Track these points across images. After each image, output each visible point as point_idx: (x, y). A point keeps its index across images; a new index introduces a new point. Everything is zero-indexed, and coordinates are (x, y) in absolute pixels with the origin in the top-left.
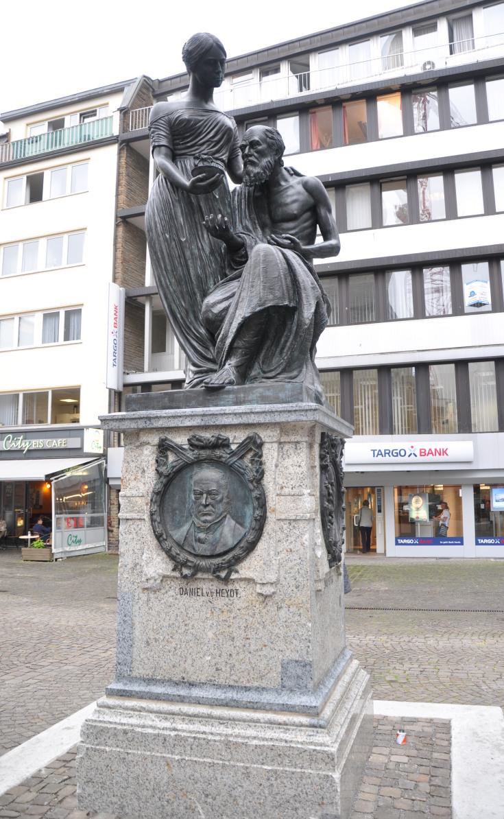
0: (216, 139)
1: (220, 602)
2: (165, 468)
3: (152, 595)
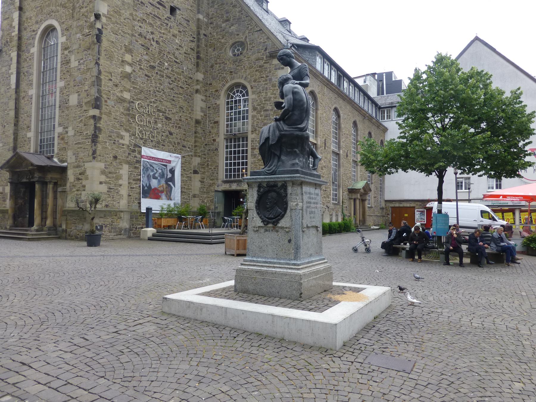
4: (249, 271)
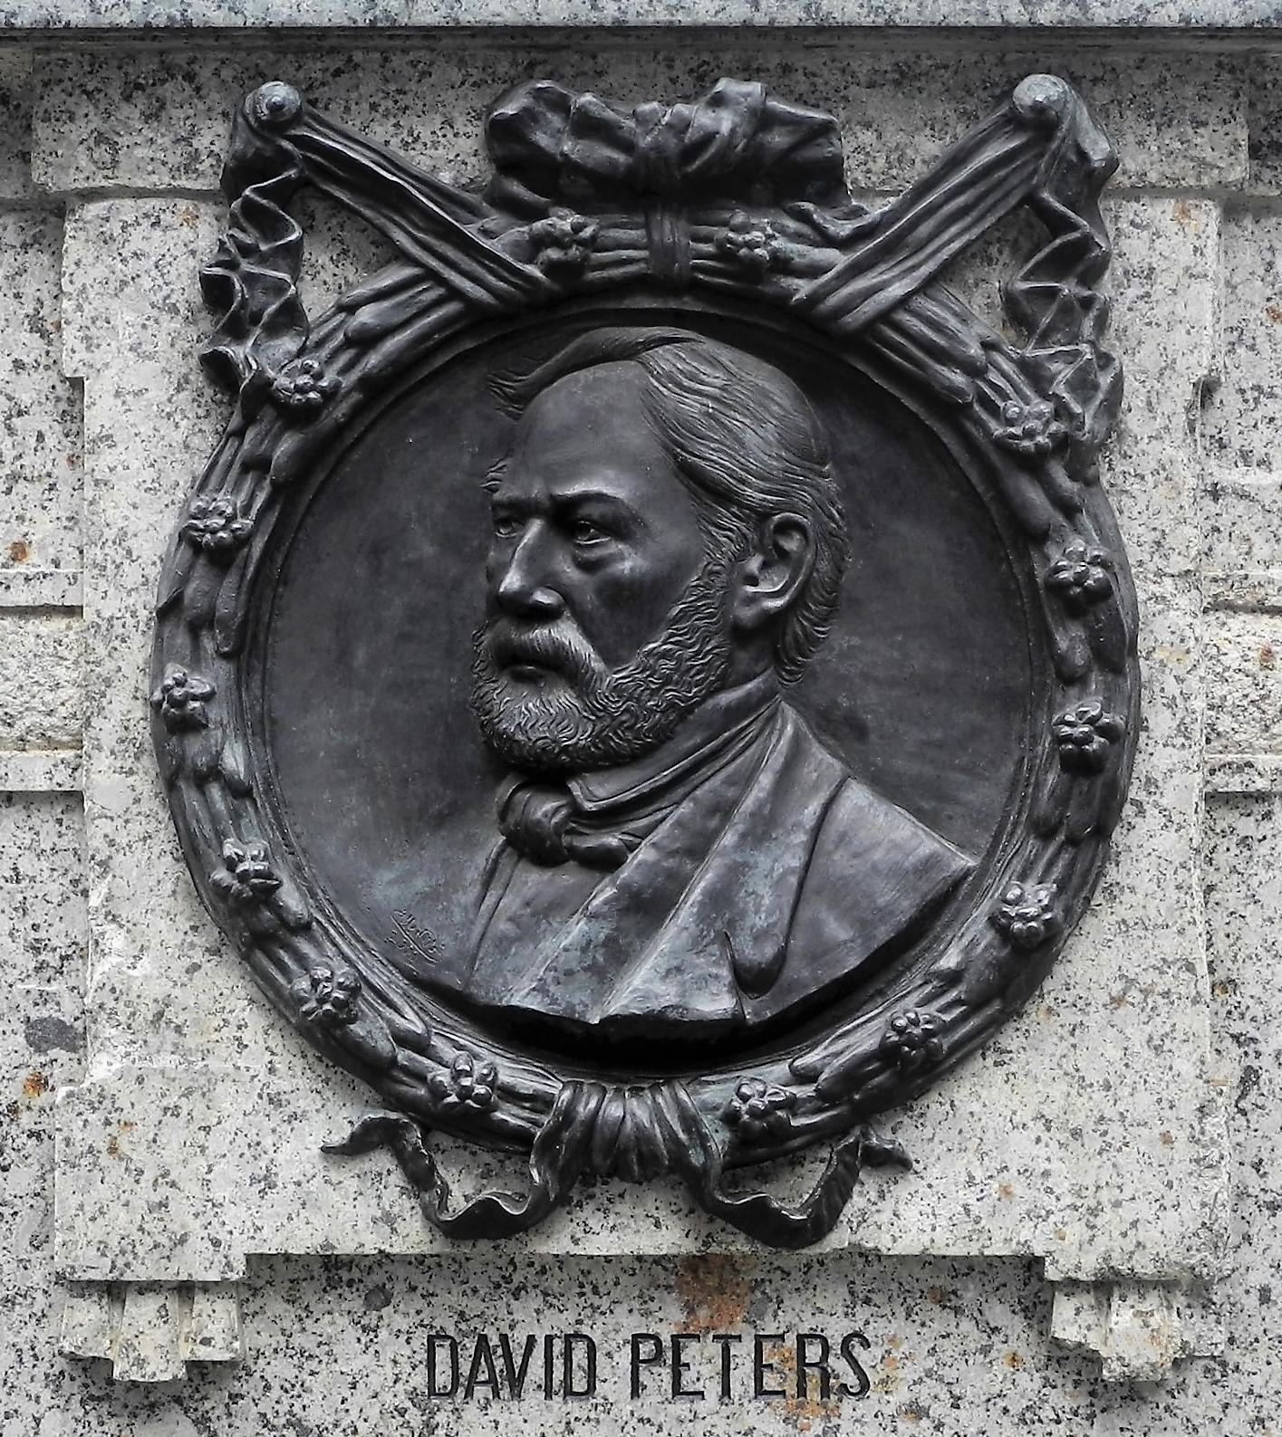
2: (289, 344)
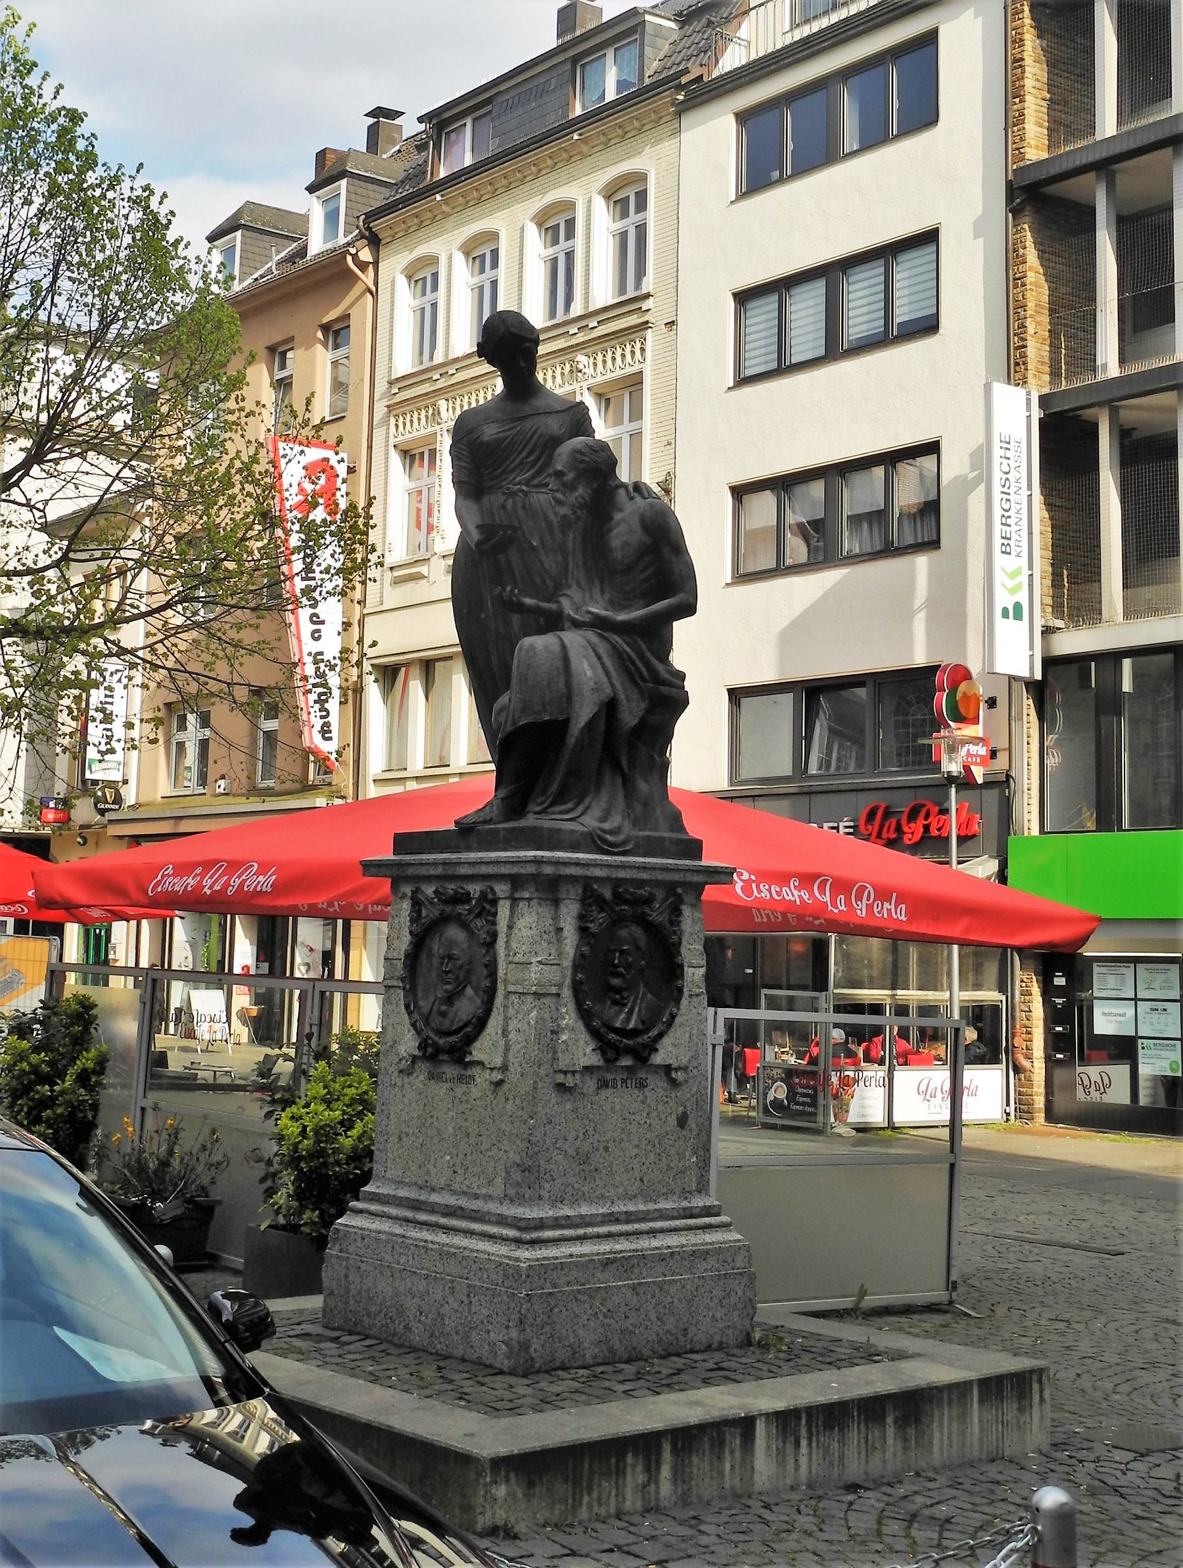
0: (531, 459)
1: (460, 1089)
3: (406, 1080)
4: (576, 1264)
